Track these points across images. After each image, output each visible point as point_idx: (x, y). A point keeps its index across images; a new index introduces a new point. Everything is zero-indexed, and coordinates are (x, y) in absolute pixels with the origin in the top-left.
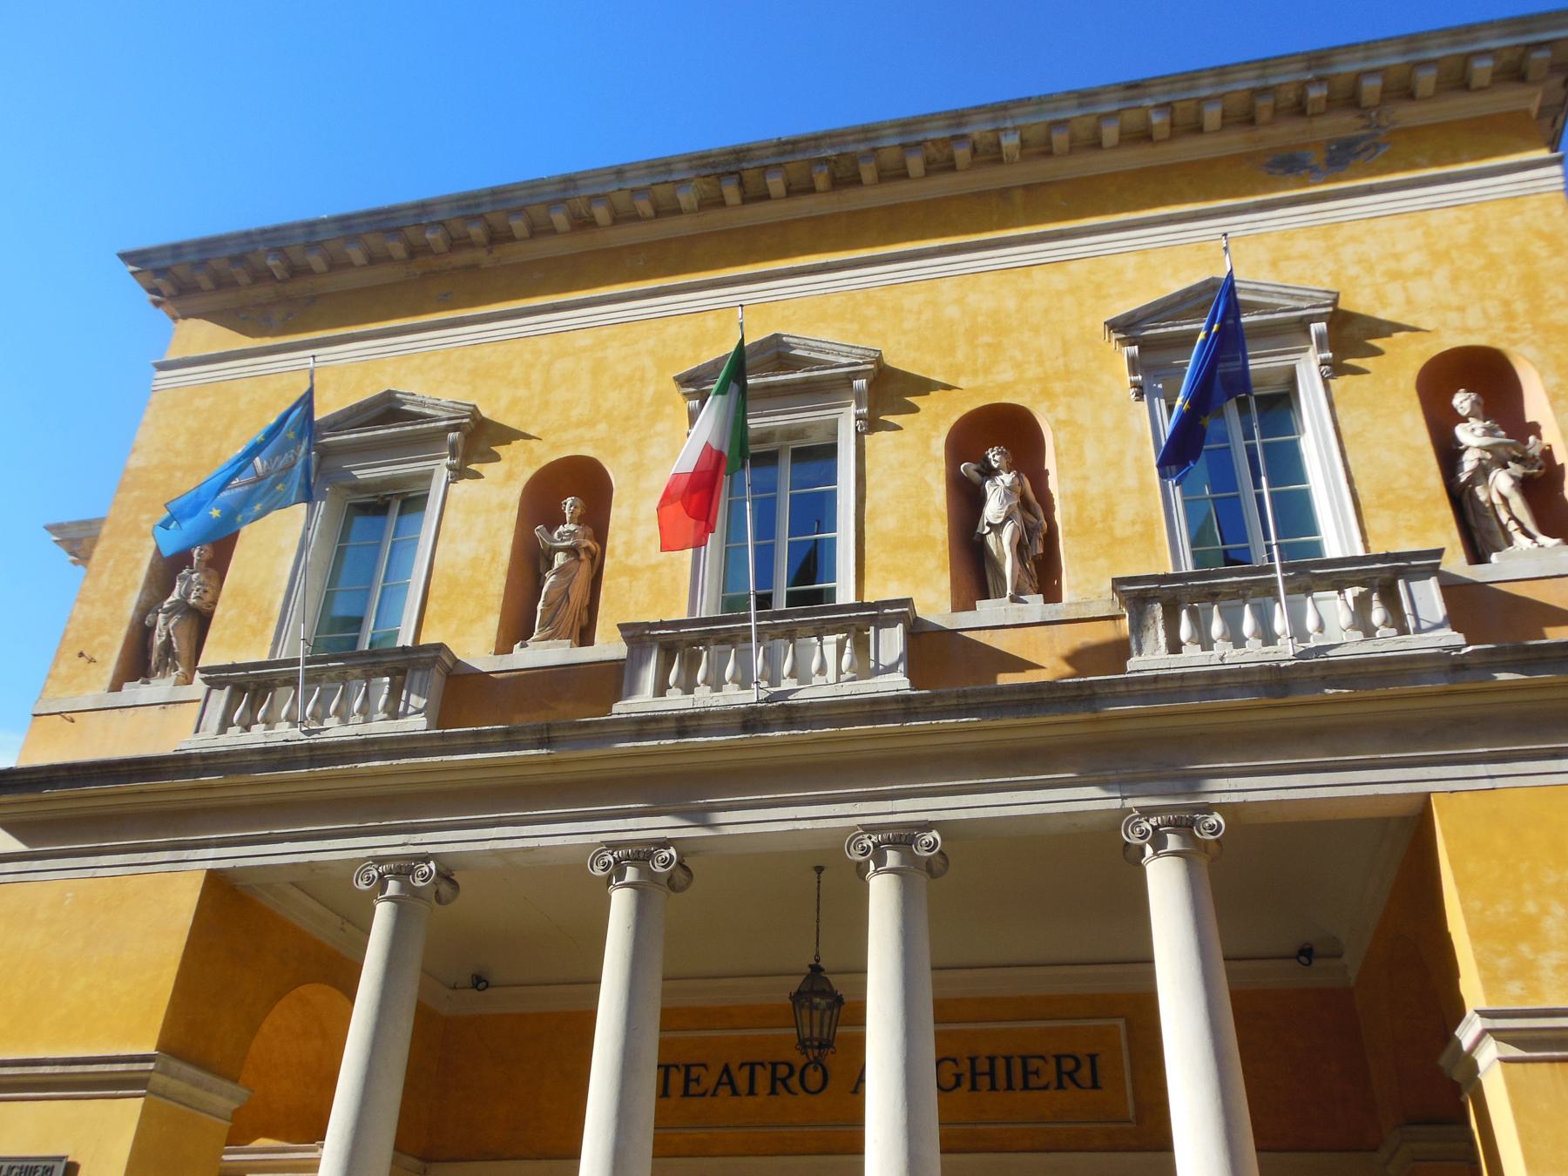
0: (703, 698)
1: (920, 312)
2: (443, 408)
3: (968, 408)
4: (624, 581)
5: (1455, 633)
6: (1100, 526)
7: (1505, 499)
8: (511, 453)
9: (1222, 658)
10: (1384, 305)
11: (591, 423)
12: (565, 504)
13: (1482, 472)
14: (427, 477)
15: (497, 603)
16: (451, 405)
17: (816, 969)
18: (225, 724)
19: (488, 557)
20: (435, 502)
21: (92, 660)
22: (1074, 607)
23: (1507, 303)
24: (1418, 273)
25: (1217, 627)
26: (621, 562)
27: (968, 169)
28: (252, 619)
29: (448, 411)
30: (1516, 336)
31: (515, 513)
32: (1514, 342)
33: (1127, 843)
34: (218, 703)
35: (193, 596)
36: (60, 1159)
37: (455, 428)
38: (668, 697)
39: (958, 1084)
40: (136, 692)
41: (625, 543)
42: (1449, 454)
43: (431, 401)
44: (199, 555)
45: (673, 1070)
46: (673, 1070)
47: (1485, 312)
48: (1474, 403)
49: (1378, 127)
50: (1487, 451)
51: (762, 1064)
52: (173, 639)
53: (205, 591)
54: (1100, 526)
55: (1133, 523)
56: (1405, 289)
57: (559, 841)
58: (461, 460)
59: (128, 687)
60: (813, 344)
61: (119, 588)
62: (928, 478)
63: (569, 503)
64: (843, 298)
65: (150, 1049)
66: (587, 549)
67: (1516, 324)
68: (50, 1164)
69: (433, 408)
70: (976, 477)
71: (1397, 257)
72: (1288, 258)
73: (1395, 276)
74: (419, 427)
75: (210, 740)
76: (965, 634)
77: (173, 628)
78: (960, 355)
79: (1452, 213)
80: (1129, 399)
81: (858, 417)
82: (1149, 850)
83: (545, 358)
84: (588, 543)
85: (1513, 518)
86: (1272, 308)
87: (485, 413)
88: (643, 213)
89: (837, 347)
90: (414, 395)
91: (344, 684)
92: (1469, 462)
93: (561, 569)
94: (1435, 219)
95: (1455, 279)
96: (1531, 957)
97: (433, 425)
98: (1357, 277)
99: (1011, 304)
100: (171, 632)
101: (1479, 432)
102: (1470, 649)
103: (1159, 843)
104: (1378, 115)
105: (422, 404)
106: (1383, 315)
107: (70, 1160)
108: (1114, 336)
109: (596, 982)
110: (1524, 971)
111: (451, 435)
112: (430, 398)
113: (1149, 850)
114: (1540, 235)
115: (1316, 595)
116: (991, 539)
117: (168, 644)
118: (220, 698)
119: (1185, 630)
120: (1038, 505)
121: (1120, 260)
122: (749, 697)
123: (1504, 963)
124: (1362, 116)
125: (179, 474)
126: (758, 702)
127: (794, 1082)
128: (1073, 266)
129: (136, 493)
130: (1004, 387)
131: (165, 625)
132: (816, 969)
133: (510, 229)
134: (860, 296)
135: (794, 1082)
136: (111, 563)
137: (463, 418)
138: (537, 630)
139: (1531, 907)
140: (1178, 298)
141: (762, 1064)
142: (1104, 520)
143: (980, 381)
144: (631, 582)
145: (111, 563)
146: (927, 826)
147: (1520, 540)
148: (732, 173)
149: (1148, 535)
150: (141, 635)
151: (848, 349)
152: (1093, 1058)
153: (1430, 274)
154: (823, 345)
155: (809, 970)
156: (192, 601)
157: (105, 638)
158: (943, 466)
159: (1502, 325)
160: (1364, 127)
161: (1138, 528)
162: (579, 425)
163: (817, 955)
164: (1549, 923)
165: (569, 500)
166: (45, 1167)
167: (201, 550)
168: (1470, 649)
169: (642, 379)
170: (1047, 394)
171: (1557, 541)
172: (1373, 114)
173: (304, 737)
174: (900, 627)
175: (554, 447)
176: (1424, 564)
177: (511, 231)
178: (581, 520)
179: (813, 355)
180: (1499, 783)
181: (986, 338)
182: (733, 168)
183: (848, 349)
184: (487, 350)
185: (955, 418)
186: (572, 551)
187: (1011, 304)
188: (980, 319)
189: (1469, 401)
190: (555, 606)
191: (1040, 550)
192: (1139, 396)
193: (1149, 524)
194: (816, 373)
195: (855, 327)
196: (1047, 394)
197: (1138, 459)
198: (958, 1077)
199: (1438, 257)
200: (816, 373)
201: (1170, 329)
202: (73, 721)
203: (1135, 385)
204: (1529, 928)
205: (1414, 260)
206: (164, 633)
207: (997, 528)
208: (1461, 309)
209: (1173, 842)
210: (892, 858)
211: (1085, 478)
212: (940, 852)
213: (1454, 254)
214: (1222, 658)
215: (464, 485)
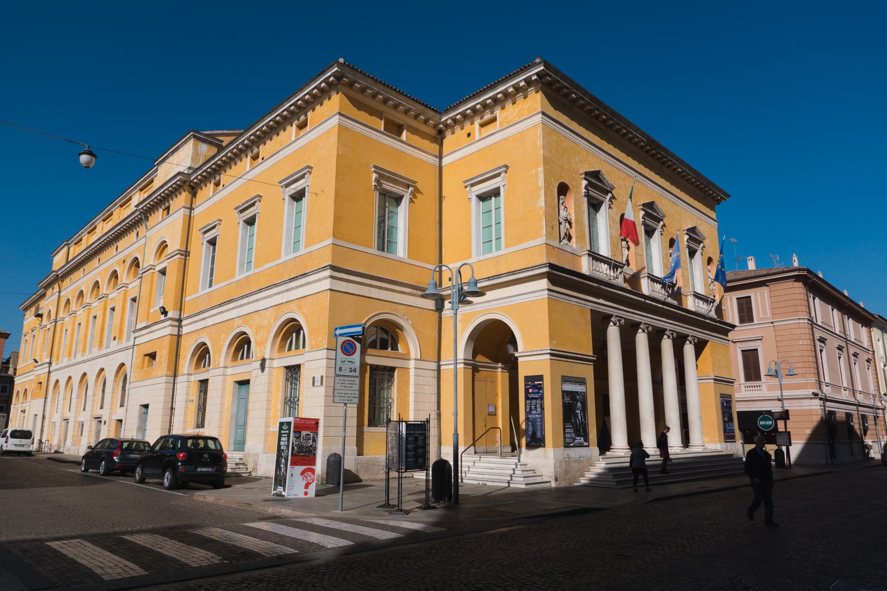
86: (698, 236)
105: (604, 179)
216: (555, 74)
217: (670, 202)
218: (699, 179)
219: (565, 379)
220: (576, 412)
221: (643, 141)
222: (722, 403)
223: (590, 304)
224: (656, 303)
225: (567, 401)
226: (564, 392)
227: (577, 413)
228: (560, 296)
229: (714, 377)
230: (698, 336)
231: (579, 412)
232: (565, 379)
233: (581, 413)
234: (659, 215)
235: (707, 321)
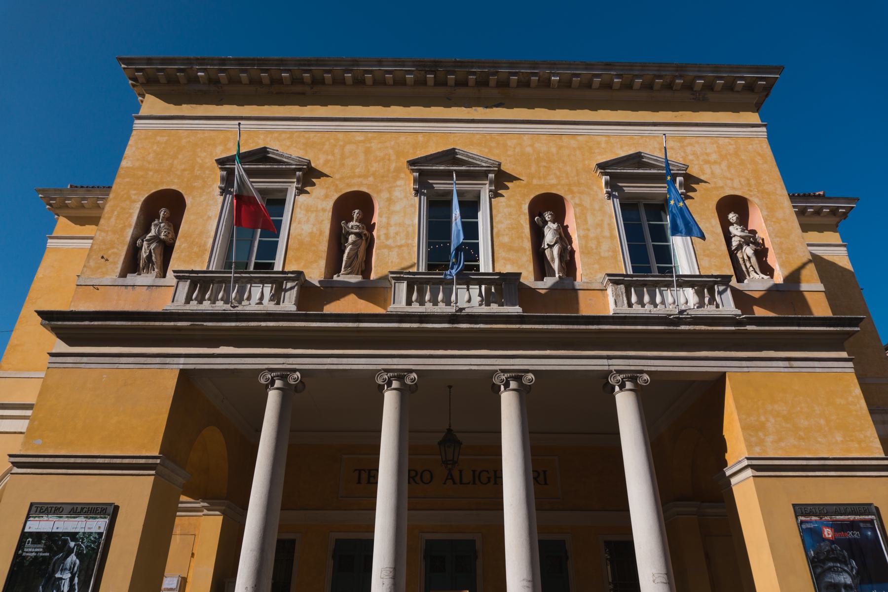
0: (428, 308)
1: (515, 148)
2: (293, 159)
3: (538, 193)
4: (385, 251)
5: (737, 309)
6: (595, 251)
7: (749, 258)
8: (327, 186)
9: (650, 311)
10: (704, 174)
11: (365, 176)
12: (355, 212)
13: (740, 247)
14: (285, 191)
15: (324, 255)
16: (298, 158)
17: (449, 430)
18: (188, 300)
19: (318, 233)
20: (289, 204)
21: (107, 260)
22: (586, 284)
23: (748, 180)
24: (715, 162)
25: (646, 298)
26: (383, 243)
27: (516, 88)
28: (196, 249)
29: (296, 161)
30: (752, 193)
31: (330, 214)
32: (751, 196)
33: (494, 383)
34: (184, 289)
35: (162, 234)
36: (111, 504)
37: (299, 170)
38: (413, 306)
39: (489, 481)
40: (131, 279)
41: (385, 234)
42: (728, 238)
43: (287, 155)
44: (164, 214)
45: (363, 472)
46: (363, 472)
47: (740, 182)
48: (737, 218)
50: (742, 238)
51: (364, 470)
52: (153, 255)
53: (169, 233)
54: (595, 251)
55: (608, 251)
56: (711, 168)
57: (361, 367)
58: (302, 185)
59: (129, 276)
60: (471, 155)
61: (120, 226)
62: (522, 222)
63: (356, 212)
64: (481, 136)
65: (156, 454)
66: (365, 235)
67: (752, 189)
68: (105, 507)
69: (287, 159)
70: (541, 224)
71: (708, 154)
73: (707, 162)
74: (281, 167)
75: (179, 305)
76: (538, 290)
77: (153, 249)
78: (533, 169)
79: (727, 140)
80: (604, 198)
81: (490, 191)
82: (502, 388)
83: (341, 143)
84: (366, 232)
85: (752, 266)
87: (313, 165)
88: (388, 83)
89: (482, 158)
90: (278, 151)
91: (225, 284)
92: (735, 242)
93: (353, 243)
94: (721, 141)
95: (729, 167)
96: (763, 437)
97: (288, 167)
98: (693, 160)
99: (554, 150)
100: (152, 251)
101: (740, 230)
102: (744, 316)
103: (622, 387)
104: (699, 95)
105: (282, 156)
106: (702, 178)
107: (115, 504)
108: (599, 171)
109: (379, 431)
110: (761, 442)
111: (298, 173)
112: (286, 154)
113: (502, 388)
114: (759, 154)
115: (684, 289)
116: (547, 252)
117: (149, 257)
118: (184, 287)
119: (634, 299)
120: (565, 238)
121: (599, 139)
122: (451, 310)
123: (753, 439)
125: (151, 173)
126: (456, 312)
127: (418, 479)
128: (580, 138)
129: (127, 180)
130: (553, 186)
131: (148, 247)
132: (449, 430)
133: (323, 79)
134: (488, 137)
135: (418, 479)
136: (116, 213)
137: (304, 165)
138: (343, 269)
139: (763, 419)
140: (625, 159)
141: (364, 470)
142: (596, 249)
143: (542, 182)
144: (389, 252)
145: (116, 213)
146: (410, 371)
147: (753, 274)
148: (432, 71)
149: (615, 258)
150: (134, 251)
151: (487, 160)
152: (545, 472)
153: (720, 164)
154: (475, 156)
155: (446, 431)
156: (162, 236)
157: (115, 250)
158: (528, 217)
159: (747, 188)
160: (693, 99)
161: (610, 253)
162: (359, 177)
163: (450, 424)
164: (769, 425)
165: (357, 211)
166: (102, 508)
167: (165, 212)
168: (744, 316)
169: (389, 160)
170: (571, 192)
171: (768, 277)
173: (232, 309)
174: (406, 282)
175: (348, 185)
176: (725, 280)
177: (345, 80)
178: (360, 220)
179: (470, 160)
180: (751, 370)
181: (544, 164)
182: (433, 69)
183: (487, 160)
184: (312, 135)
185: (532, 197)
186: (357, 235)
187: (554, 150)
188: (541, 155)
189: (735, 217)
190: (351, 259)
191: (568, 258)
192: (609, 198)
193: (615, 251)
194: (472, 168)
195: (487, 150)
196: (571, 192)
197: (609, 225)
198: (489, 478)
200: (472, 168)
201: (622, 171)
202: (98, 289)
203: (607, 192)
204: (762, 427)
205: (714, 157)
206: (148, 251)
207: (551, 246)
208: (732, 180)
209: (629, 385)
210: (395, 384)
211: (588, 230)
212: (416, 384)
213: (729, 157)
214: (650, 311)
215: (302, 198)
216: (147, 64)
218: (636, 73)
219: (38, 509)
220: (58, 575)
221: (409, 72)
222: (810, 536)
223: (182, 360)
224: (421, 322)
225: (34, 554)
226: (24, 536)
227: (61, 579)
228: (85, 359)
229: (746, 463)
230: (646, 369)
231: (67, 576)
232: (38, 509)
233: (72, 580)
234: (479, 166)
235: (683, 327)
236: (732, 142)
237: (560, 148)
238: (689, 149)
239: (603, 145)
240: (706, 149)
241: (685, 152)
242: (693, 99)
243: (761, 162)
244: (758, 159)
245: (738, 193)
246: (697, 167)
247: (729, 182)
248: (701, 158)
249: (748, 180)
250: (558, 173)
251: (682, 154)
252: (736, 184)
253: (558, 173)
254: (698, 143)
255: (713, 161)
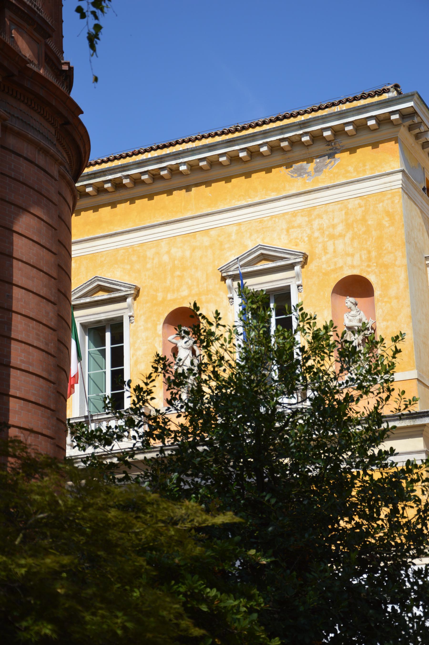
1: (153, 259)
3: (171, 310)
23: (369, 252)
32: (369, 273)
49: (336, 149)
67: (371, 263)
72: (293, 227)
73: (332, 237)
104: (335, 144)
124: (328, 145)
153: (344, 236)
160: (330, 150)
172: (333, 144)
181: (178, 273)
199: (349, 226)
208: (353, 255)
213: (355, 225)
217: (179, 239)
236: (362, 203)
237: (193, 249)
238: (316, 224)
239: (233, 237)
240: (333, 220)
241: (311, 229)
242: (330, 150)
243: (387, 225)
244: (386, 222)
245: (356, 272)
246: (320, 246)
247: (349, 259)
248: (327, 233)
249: (369, 252)
250: (190, 282)
251: (309, 232)
252: (356, 261)
253: (190, 282)
254: (326, 212)
255: (338, 234)
